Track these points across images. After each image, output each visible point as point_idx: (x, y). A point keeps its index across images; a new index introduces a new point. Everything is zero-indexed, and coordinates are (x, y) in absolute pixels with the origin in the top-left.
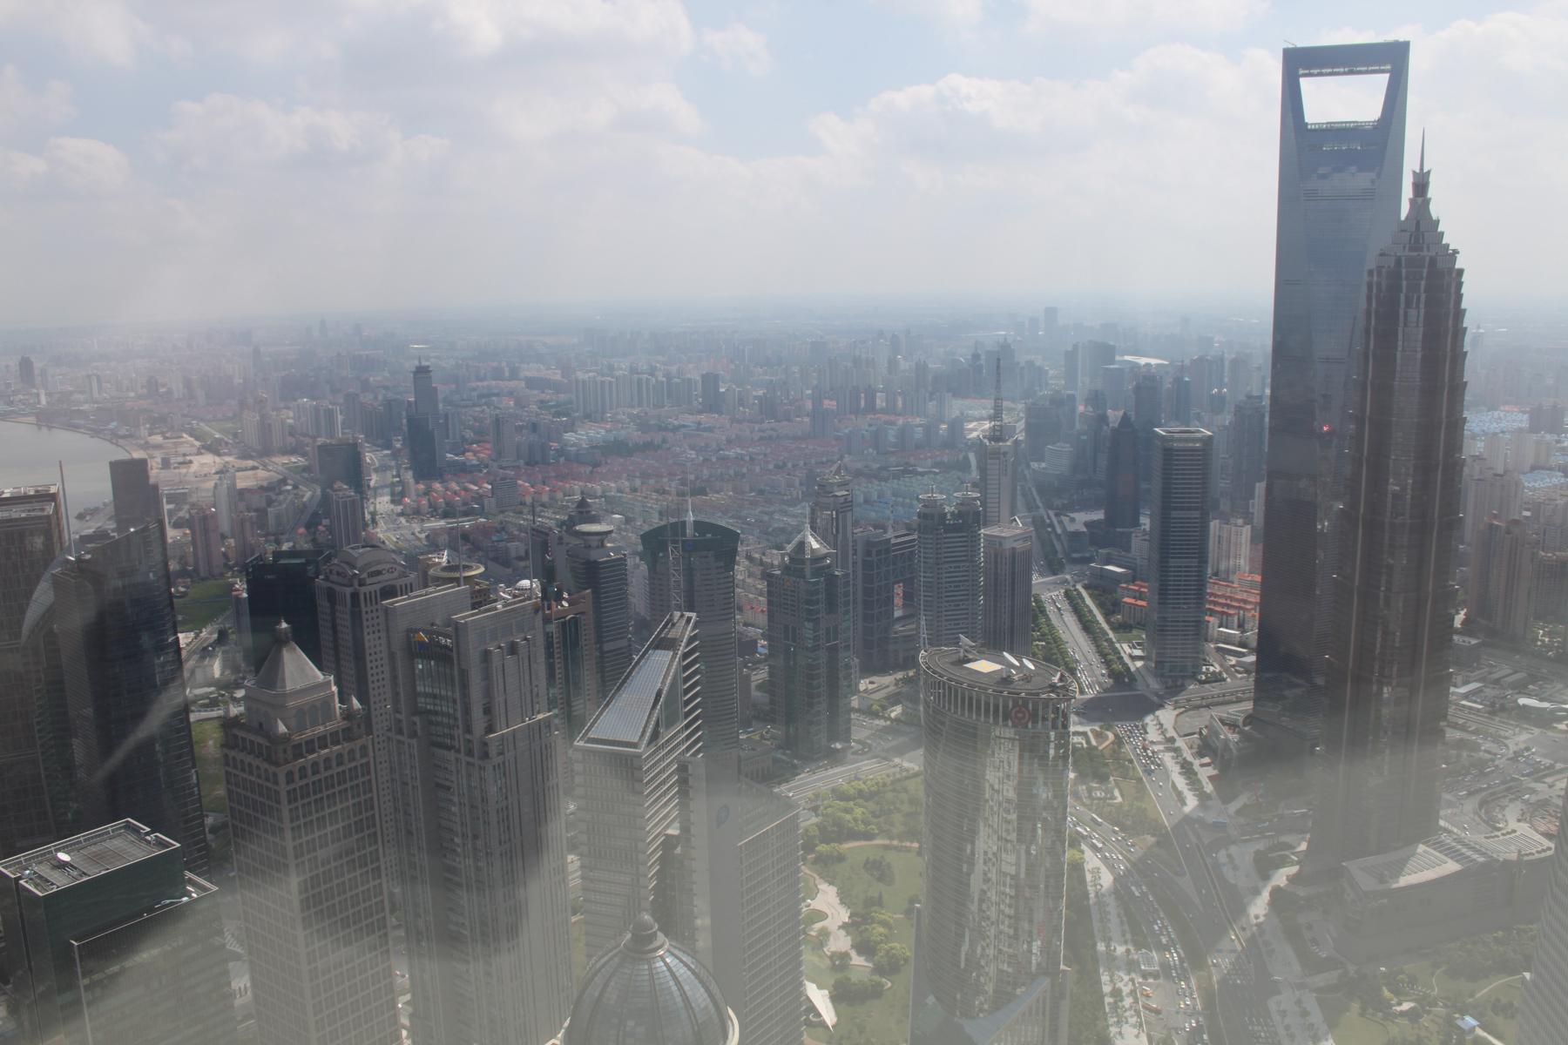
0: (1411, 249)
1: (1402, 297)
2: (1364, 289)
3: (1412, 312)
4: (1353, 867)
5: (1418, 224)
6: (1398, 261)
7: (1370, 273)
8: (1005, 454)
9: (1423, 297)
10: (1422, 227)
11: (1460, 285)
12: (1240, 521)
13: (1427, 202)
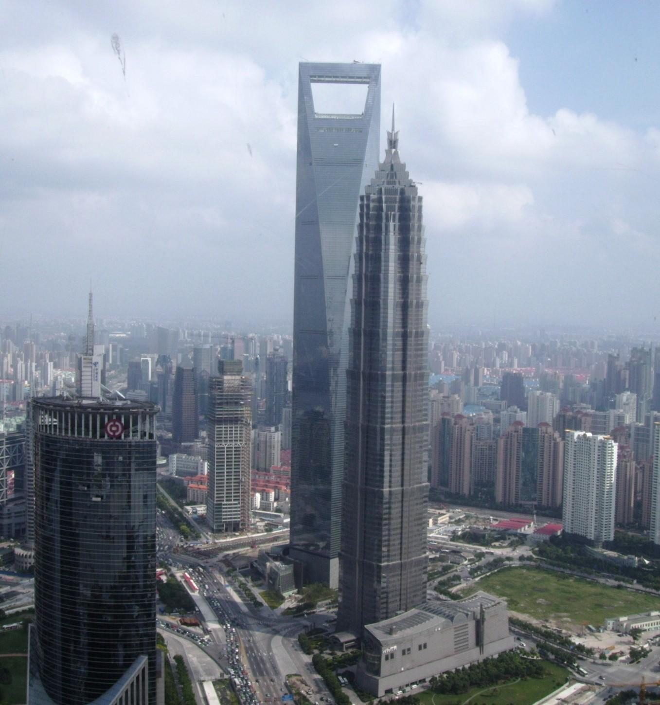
0: (388, 183)
1: (384, 214)
2: (358, 210)
3: (391, 224)
4: (369, 627)
5: (392, 166)
6: (380, 192)
7: (362, 198)
8: (96, 364)
9: (397, 214)
10: (393, 170)
11: (420, 208)
12: (273, 429)
13: (396, 153)
